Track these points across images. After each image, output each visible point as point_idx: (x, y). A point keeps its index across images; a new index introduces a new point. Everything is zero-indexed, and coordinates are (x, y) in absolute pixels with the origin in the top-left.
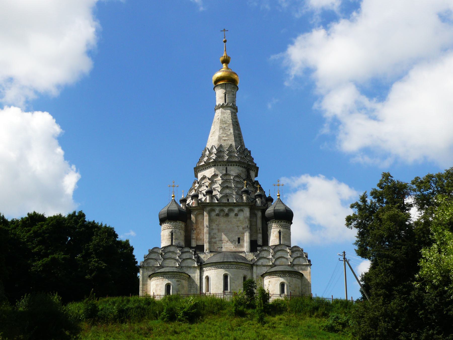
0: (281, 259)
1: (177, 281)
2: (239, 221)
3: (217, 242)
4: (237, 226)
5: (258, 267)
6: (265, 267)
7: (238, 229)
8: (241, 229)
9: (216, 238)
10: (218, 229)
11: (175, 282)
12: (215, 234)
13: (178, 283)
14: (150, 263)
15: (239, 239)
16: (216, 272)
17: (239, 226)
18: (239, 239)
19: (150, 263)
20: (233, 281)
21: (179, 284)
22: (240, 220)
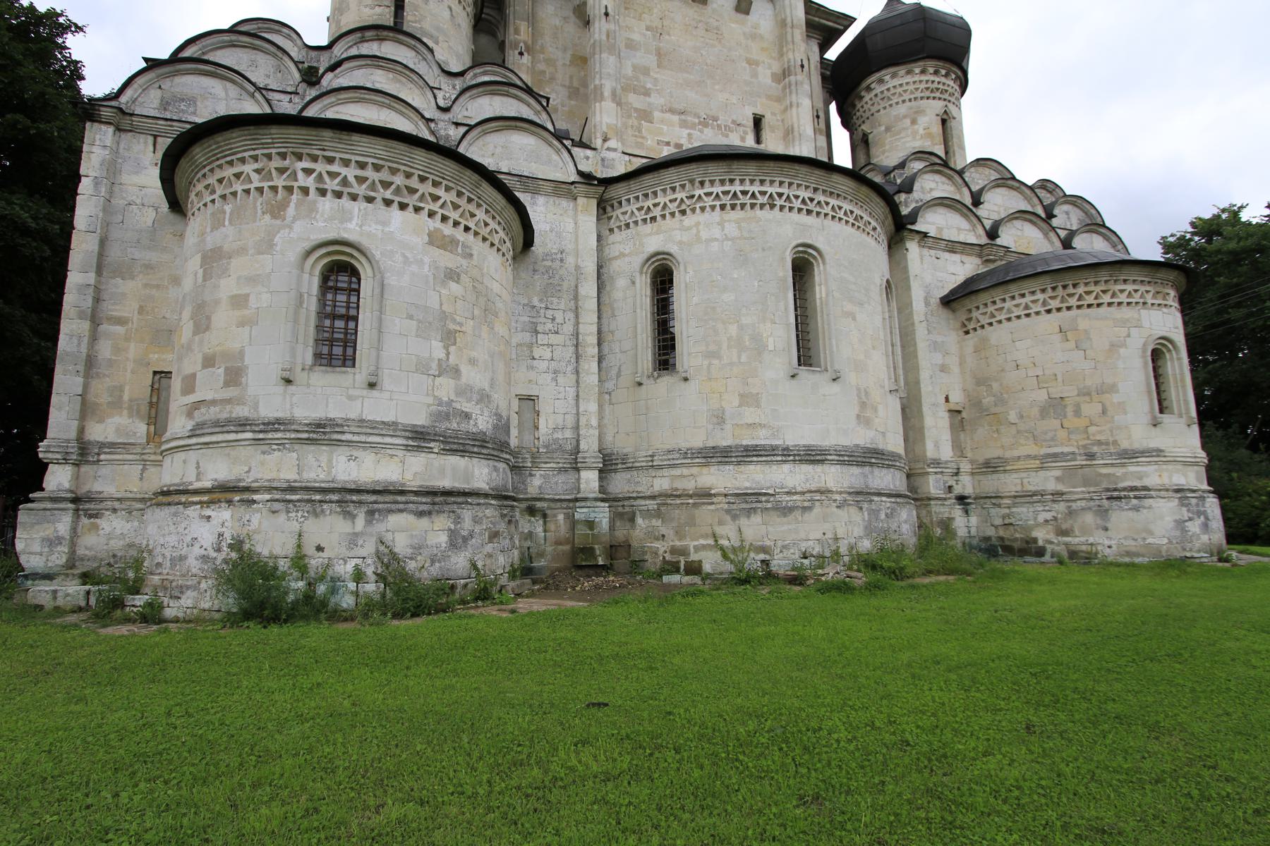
0: (1018, 223)
1: (435, 240)
2: (754, 37)
3: (657, 114)
4: (750, 62)
5: (925, 251)
6: (957, 257)
7: (755, 75)
8: (765, 76)
9: (647, 93)
10: (659, 54)
11: (420, 240)
12: (646, 71)
13: (447, 260)
14: (192, 101)
15: (758, 122)
16: (731, 229)
17: (757, 63)
18: (758, 122)
19: (192, 101)
20: (849, 307)
21: (452, 275)
22: (762, 37)
